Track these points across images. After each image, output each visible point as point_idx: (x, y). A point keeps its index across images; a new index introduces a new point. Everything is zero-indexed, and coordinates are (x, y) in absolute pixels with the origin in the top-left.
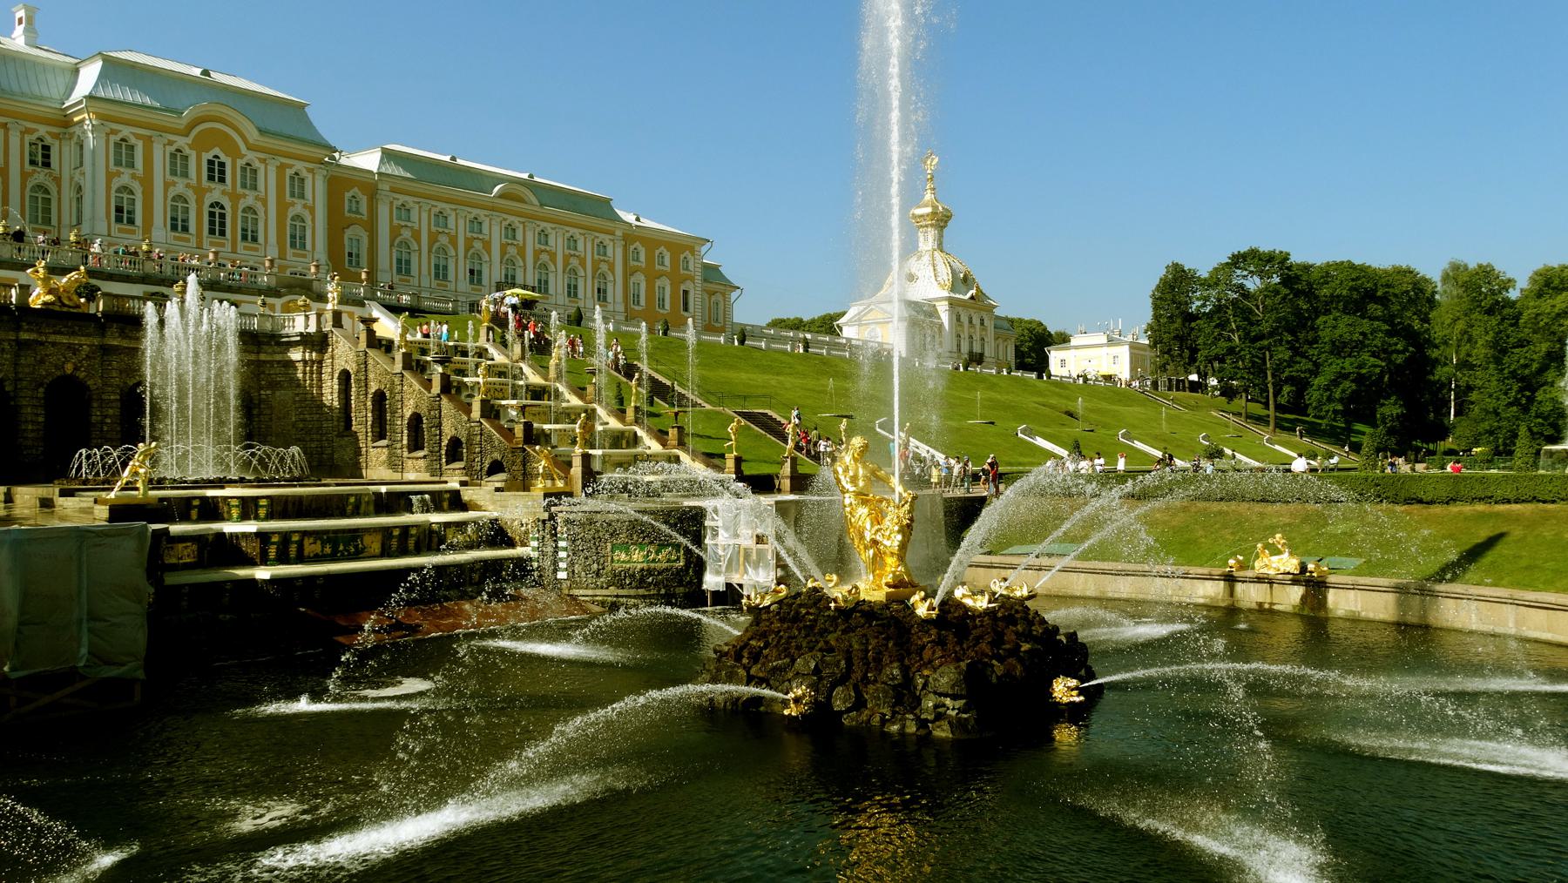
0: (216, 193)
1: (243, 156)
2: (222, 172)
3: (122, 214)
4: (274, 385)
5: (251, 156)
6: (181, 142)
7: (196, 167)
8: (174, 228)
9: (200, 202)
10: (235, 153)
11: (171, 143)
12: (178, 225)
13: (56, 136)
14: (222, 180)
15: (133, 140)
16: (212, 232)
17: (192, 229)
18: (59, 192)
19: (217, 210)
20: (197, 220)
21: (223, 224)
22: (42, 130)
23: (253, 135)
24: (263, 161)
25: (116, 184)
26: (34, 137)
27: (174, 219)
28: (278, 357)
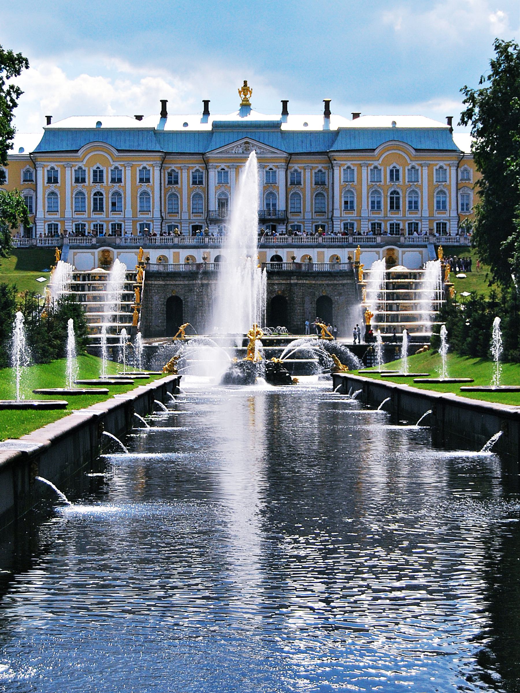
3: (348, 205)
4: (340, 294)
5: (414, 163)
8: (373, 207)
11: (370, 165)
12: (375, 206)
13: (325, 168)
14: (398, 179)
16: (392, 207)
18: (328, 195)
19: (395, 196)
21: (398, 203)
23: (413, 152)
24: (421, 165)
27: (373, 202)
28: (341, 282)
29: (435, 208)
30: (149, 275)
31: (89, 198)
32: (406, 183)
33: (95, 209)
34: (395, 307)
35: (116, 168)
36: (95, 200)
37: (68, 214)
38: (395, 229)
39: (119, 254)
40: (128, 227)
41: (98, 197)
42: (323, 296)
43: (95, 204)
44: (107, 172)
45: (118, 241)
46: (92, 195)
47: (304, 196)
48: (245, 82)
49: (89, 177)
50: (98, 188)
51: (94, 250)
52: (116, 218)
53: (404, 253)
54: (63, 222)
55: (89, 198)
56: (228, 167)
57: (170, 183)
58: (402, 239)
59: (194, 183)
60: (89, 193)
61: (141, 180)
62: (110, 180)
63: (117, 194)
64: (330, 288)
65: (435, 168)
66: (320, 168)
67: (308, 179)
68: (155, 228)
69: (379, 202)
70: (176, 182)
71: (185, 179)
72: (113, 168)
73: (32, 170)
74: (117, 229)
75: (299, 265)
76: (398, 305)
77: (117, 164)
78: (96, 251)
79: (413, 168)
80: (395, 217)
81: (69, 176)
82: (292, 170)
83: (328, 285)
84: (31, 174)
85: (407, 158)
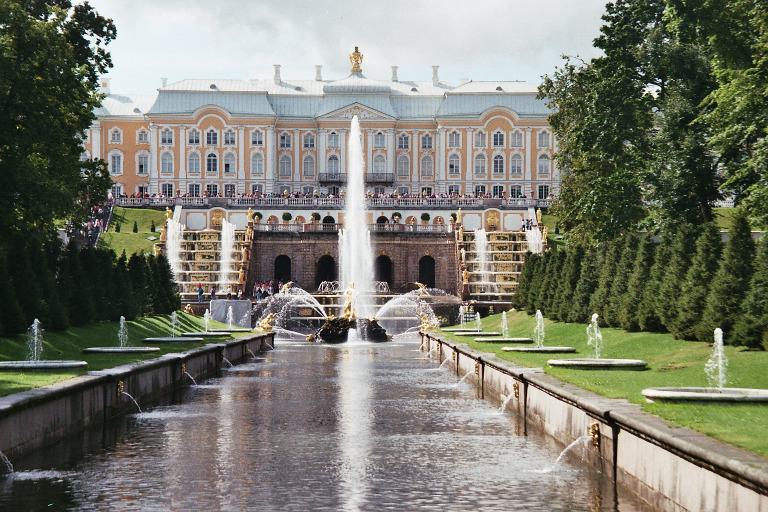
0: (498, 151)
1: (512, 129)
2: (502, 140)
4: (442, 255)
6: (480, 128)
7: (489, 140)
8: (477, 171)
9: (489, 157)
10: (509, 129)
11: (475, 130)
12: (479, 171)
13: (432, 133)
14: (502, 143)
15: (458, 132)
16: (496, 171)
17: (486, 171)
20: (488, 165)
21: (501, 167)
22: (427, 131)
24: (523, 130)
25: (450, 154)
26: (424, 135)
29: (538, 171)
30: (258, 235)
31: (203, 160)
32: (510, 148)
33: (209, 169)
34: (493, 267)
35: (230, 131)
36: (209, 160)
37: (182, 174)
38: (498, 190)
39: (230, 214)
40: (240, 188)
41: (212, 158)
42: (429, 257)
43: (209, 165)
44: (221, 136)
45: (230, 201)
46: (206, 158)
47: (412, 159)
48: (356, 48)
49: (203, 139)
50: (211, 150)
51: (205, 210)
52: (229, 179)
53: (505, 215)
54: (177, 183)
55: (203, 160)
56: (338, 131)
57: (283, 145)
58: (504, 202)
59: (306, 146)
60: (203, 155)
61: (254, 143)
62: (224, 142)
63: (230, 155)
64: (432, 249)
65: (538, 133)
66: (427, 132)
67: (415, 142)
68: (268, 189)
69: (483, 168)
70: (288, 146)
71: (297, 141)
72: (226, 131)
73: (146, 130)
74: (230, 189)
75: (402, 226)
76: (496, 265)
77: (230, 127)
78: (208, 211)
79: (517, 132)
80: (498, 180)
81: (184, 137)
82: (400, 135)
83: (430, 246)
84: (146, 135)
85: (512, 124)
